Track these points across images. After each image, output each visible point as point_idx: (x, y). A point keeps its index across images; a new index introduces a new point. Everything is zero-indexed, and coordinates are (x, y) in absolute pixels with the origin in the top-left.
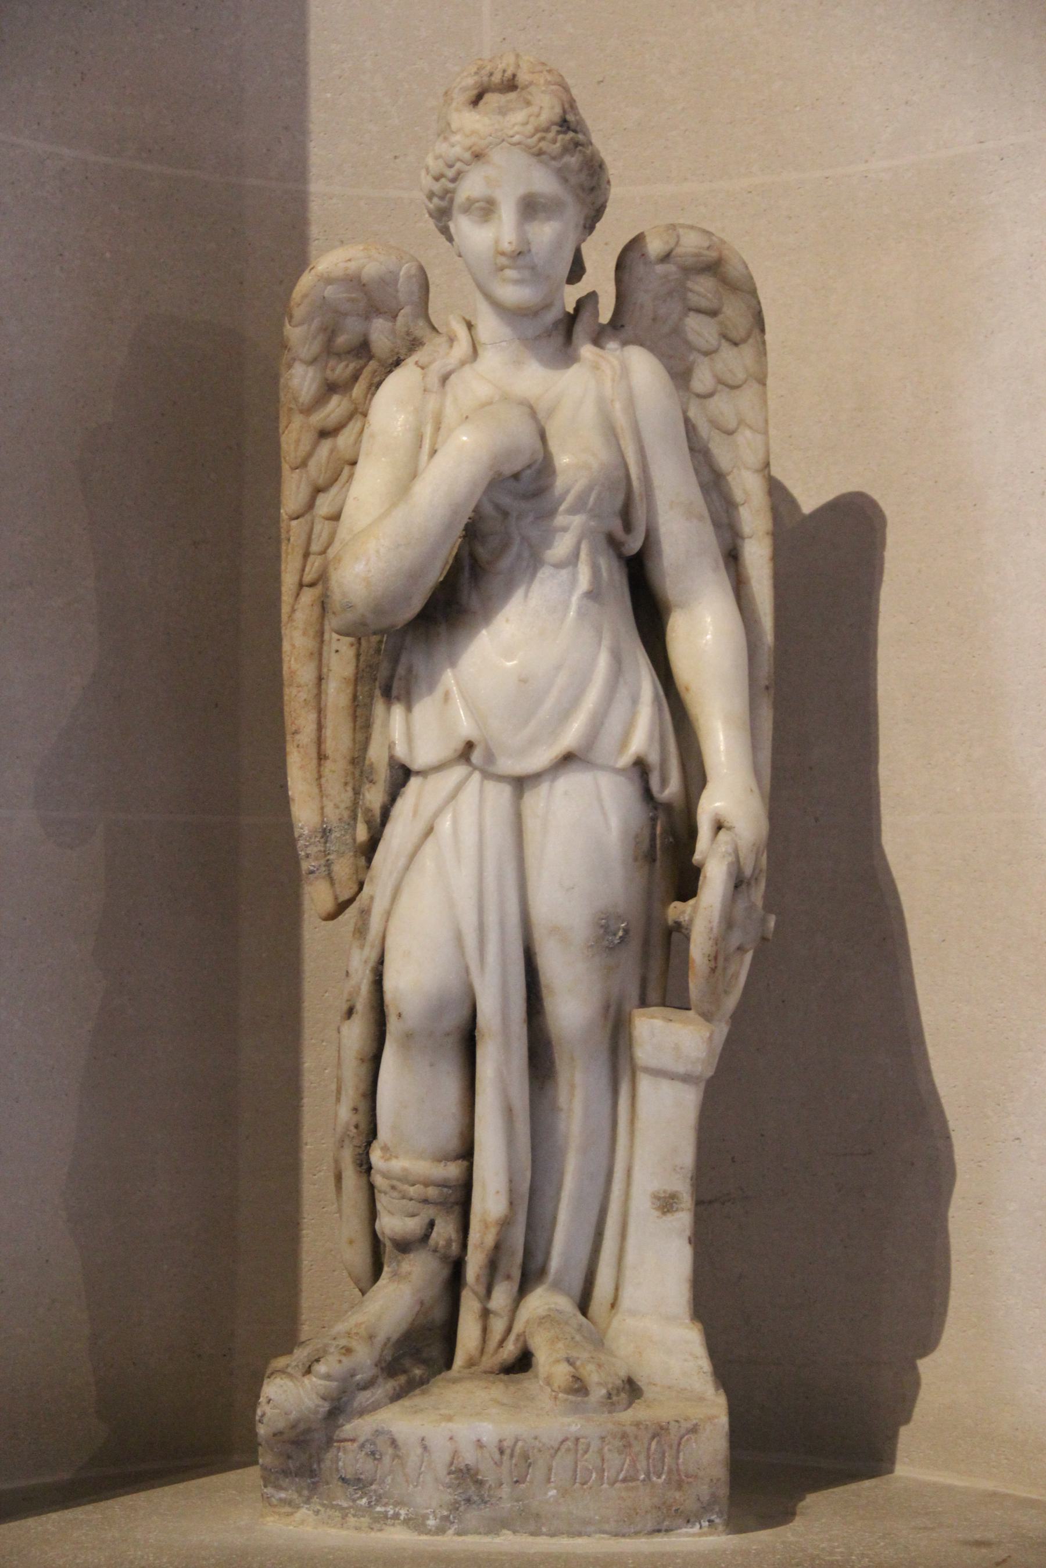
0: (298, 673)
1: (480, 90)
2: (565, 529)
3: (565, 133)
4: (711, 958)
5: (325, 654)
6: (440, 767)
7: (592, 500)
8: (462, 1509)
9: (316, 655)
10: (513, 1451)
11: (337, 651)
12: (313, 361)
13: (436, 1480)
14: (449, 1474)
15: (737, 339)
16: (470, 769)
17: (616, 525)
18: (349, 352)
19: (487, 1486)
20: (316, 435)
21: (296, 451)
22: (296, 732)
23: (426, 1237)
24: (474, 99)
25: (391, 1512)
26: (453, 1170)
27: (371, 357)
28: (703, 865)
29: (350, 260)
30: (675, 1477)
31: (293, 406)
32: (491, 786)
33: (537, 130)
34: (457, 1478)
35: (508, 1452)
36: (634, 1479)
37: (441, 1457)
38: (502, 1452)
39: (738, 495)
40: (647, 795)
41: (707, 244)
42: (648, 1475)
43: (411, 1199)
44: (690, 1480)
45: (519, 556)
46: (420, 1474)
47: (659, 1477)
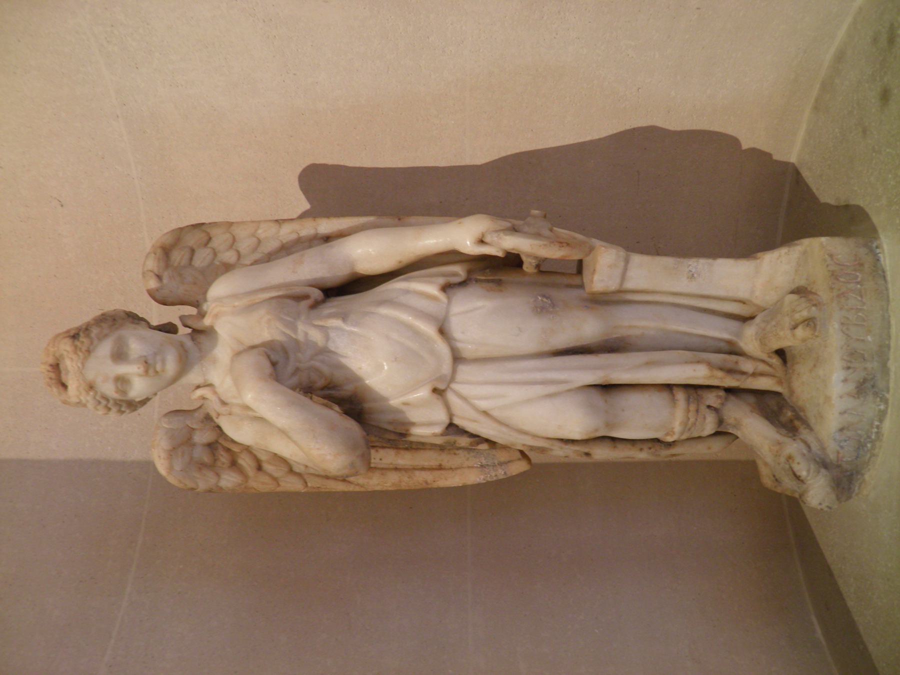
2: (306, 334)
5: (382, 466)
6: (448, 407)
7: (289, 319)
12: (218, 475)
17: (305, 304)
18: (214, 455)
22: (426, 483)
23: (716, 410)
26: (680, 396)
35: (849, 364)
37: (849, 403)
38: (849, 368)
39: (294, 236)
40: (463, 284)
41: (153, 255)
42: (858, 283)
47: (857, 277)
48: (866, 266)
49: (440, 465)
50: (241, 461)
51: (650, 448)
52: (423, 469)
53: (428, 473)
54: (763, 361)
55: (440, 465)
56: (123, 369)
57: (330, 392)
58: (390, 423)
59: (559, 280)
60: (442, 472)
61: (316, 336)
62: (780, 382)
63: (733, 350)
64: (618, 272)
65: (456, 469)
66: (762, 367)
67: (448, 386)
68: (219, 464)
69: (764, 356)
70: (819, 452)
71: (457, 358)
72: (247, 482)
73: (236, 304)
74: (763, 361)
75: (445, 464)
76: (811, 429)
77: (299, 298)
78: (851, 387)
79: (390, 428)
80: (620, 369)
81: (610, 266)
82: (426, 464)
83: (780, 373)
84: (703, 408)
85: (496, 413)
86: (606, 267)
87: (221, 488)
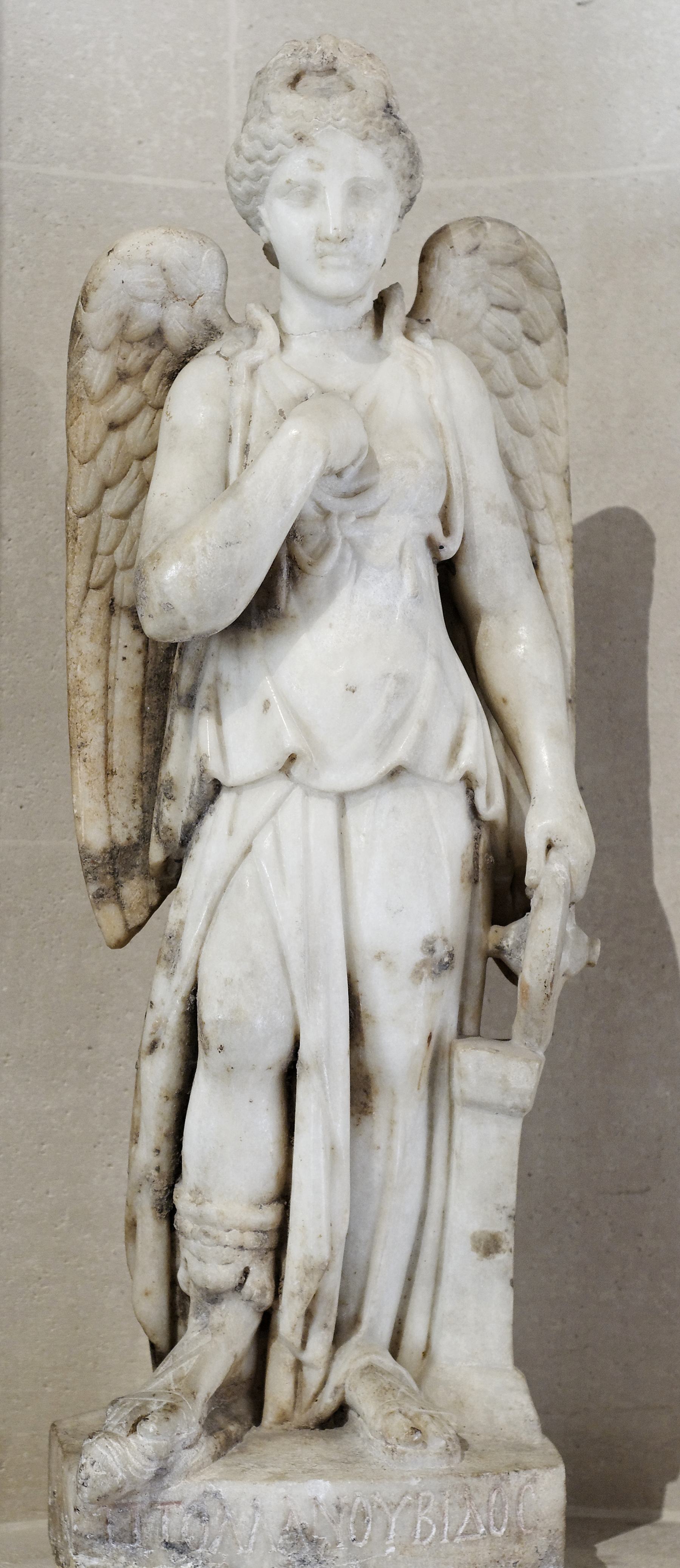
0: (86, 682)
9: (103, 662)
12: (107, 348)
14: (282, 1534)
18: (141, 341)
19: (323, 1545)
20: (106, 427)
21: (86, 445)
22: (83, 745)
30: (514, 1530)
32: (313, 801)
34: (291, 1538)
38: (339, 1509)
42: (487, 1528)
44: (529, 1532)
45: (342, 559)
46: (250, 1536)
47: (499, 1530)
48: (517, 1548)
49: (113, 773)
50: (125, 390)
51: (158, 1169)
52: (107, 740)
53: (101, 749)
54: (324, 1383)
55: (113, 773)
56: (333, 197)
57: (285, 570)
58: (218, 678)
59: (483, 984)
60: (102, 777)
62: (283, 1418)
64: (493, 1094)
65: (107, 803)
66: (313, 1378)
67: (297, 784)
68: (125, 349)
69: (334, 1380)
70: (181, 1464)
71: (342, 799)
72: (92, 402)
73: (436, 402)
74: (324, 1383)
75: (116, 781)
76: (217, 1456)
77: (445, 517)
78: (303, 1517)
79: (208, 678)
80: (324, 1097)
81: (504, 1080)
82: (115, 746)
83: (300, 1417)
84: (245, 1259)
85: (247, 868)
86: (503, 1074)
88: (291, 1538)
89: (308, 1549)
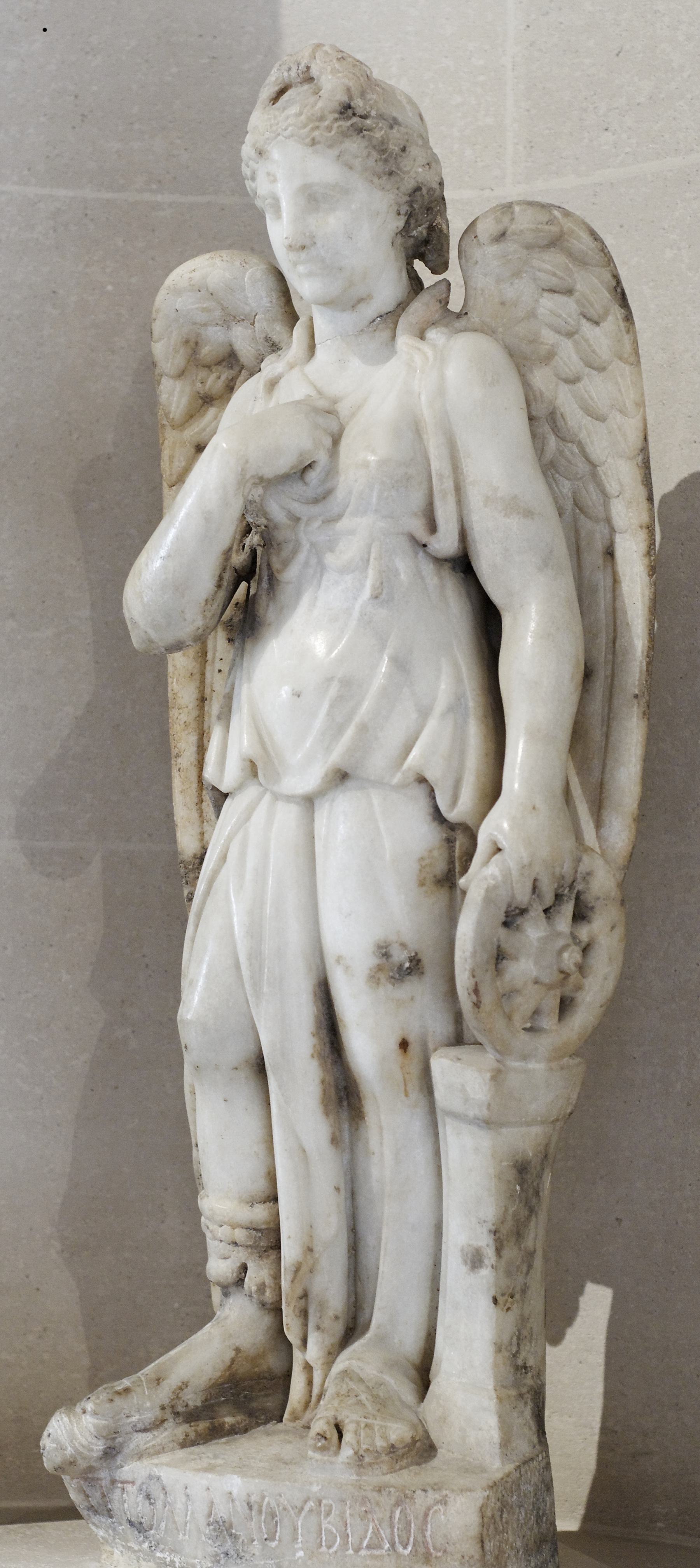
0: (179, 695)
1: (282, 86)
2: (352, 532)
3: (348, 118)
4: (471, 991)
5: (208, 675)
6: (240, 787)
7: (374, 500)
8: (222, 1562)
9: (197, 676)
10: (261, 1507)
11: (220, 671)
12: (181, 374)
13: (199, 1531)
14: (209, 1525)
15: (596, 318)
16: (261, 789)
17: (418, 527)
18: (219, 363)
19: (241, 1540)
20: (193, 450)
21: (171, 468)
22: (178, 756)
23: (240, 1282)
24: (274, 96)
25: (168, 1559)
26: (260, 1213)
27: (243, 367)
28: (467, 889)
29: (194, 271)
30: (421, 1550)
31: (165, 422)
32: (281, 806)
33: (310, 120)
34: (215, 1530)
35: (255, 1507)
36: (380, 1547)
37: (200, 1509)
38: (250, 1508)
39: (612, 487)
40: (437, 815)
41: (545, 218)
42: (393, 1545)
43: (221, 1241)
44: (439, 1554)
45: (306, 564)
46: (186, 1523)
47: (405, 1548)
57: (266, 578)
61: (349, 549)
63: (353, 1328)
68: (202, 373)
70: (132, 1446)
73: (423, 398)
76: (184, 1445)
78: (222, 1511)
81: (463, 1090)
87: (159, 383)
88: (215, 1530)
89: (229, 1542)
